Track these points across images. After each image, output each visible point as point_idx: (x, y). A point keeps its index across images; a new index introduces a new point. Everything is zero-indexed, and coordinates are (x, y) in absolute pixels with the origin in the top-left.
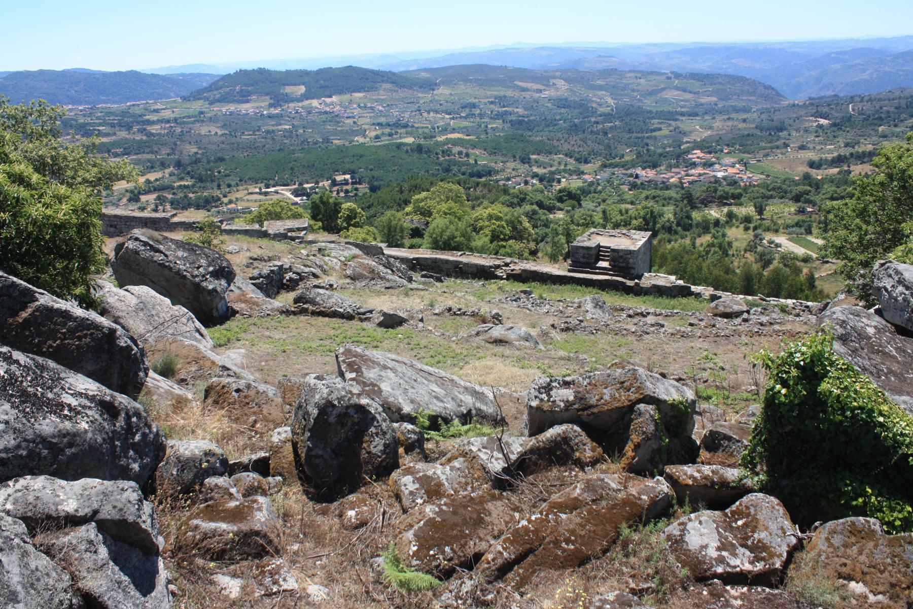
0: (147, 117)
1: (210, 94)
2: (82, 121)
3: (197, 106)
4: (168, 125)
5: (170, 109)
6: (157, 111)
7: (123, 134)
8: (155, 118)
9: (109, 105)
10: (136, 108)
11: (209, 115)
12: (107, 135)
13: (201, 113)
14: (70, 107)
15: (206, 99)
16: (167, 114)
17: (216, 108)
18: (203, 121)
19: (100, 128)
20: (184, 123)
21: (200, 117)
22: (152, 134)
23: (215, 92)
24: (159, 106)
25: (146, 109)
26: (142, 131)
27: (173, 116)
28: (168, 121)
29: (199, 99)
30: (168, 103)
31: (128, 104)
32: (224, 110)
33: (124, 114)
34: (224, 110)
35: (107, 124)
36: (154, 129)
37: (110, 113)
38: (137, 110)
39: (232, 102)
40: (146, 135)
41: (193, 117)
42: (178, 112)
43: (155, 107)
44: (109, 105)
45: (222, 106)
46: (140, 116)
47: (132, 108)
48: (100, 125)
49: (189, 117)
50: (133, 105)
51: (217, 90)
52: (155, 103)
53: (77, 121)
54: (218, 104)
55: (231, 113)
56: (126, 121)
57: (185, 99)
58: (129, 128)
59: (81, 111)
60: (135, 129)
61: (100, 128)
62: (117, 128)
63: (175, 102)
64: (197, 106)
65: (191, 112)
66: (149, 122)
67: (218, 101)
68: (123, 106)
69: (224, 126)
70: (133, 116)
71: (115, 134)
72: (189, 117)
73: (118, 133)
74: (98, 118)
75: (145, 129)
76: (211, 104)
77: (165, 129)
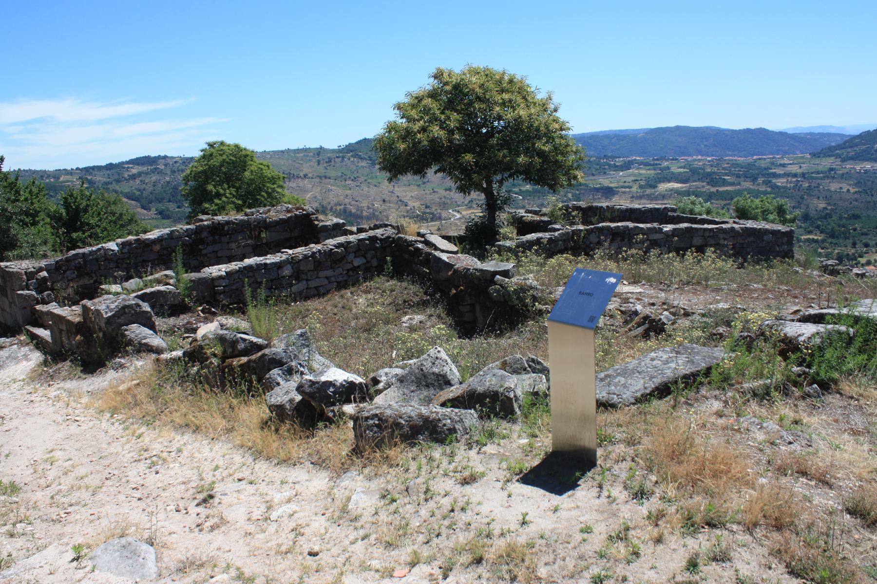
0: (773, 171)
1: (843, 151)
2: (709, 170)
3: (827, 163)
4: (794, 180)
5: (795, 164)
6: (783, 165)
7: (747, 184)
8: (782, 172)
9: (736, 158)
10: (762, 162)
11: (841, 172)
12: (732, 184)
13: (831, 169)
14: (700, 157)
15: (838, 156)
16: (794, 169)
17: (848, 166)
18: (833, 177)
19: (726, 178)
20: (812, 178)
21: (830, 174)
22: (778, 187)
23: (849, 150)
24: (786, 161)
25: (772, 163)
26: (766, 183)
27: (799, 171)
28: (795, 175)
29: (830, 156)
30: (795, 158)
31: (755, 157)
32: (858, 168)
33: (750, 166)
34: (858, 168)
35: (733, 175)
36: (780, 182)
37: (735, 165)
38: (763, 164)
39: (869, 160)
40: (771, 187)
41: (822, 172)
42: (805, 168)
43: (782, 162)
44: (736, 158)
45: (856, 164)
46: (765, 169)
47: (758, 161)
48: (726, 174)
49: (818, 173)
50: (760, 159)
51: (851, 147)
52: (782, 158)
53: (704, 169)
54: (851, 162)
55: (866, 172)
56: (751, 173)
57: (814, 155)
58: (754, 179)
59: (709, 161)
60: (760, 180)
61: (726, 178)
62: (742, 179)
63: (802, 158)
64: (827, 163)
65: (820, 168)
66: (775, 175)
67: (852, 158)
68: (749, 159)
69: (856, 185)
70: (759, 168)
71: (739, 184)
72: (818, 173)
73: (743, 183)
74: (724, 169)
75: (770, 182)
76: (843, 161)
77: (791, 183)
